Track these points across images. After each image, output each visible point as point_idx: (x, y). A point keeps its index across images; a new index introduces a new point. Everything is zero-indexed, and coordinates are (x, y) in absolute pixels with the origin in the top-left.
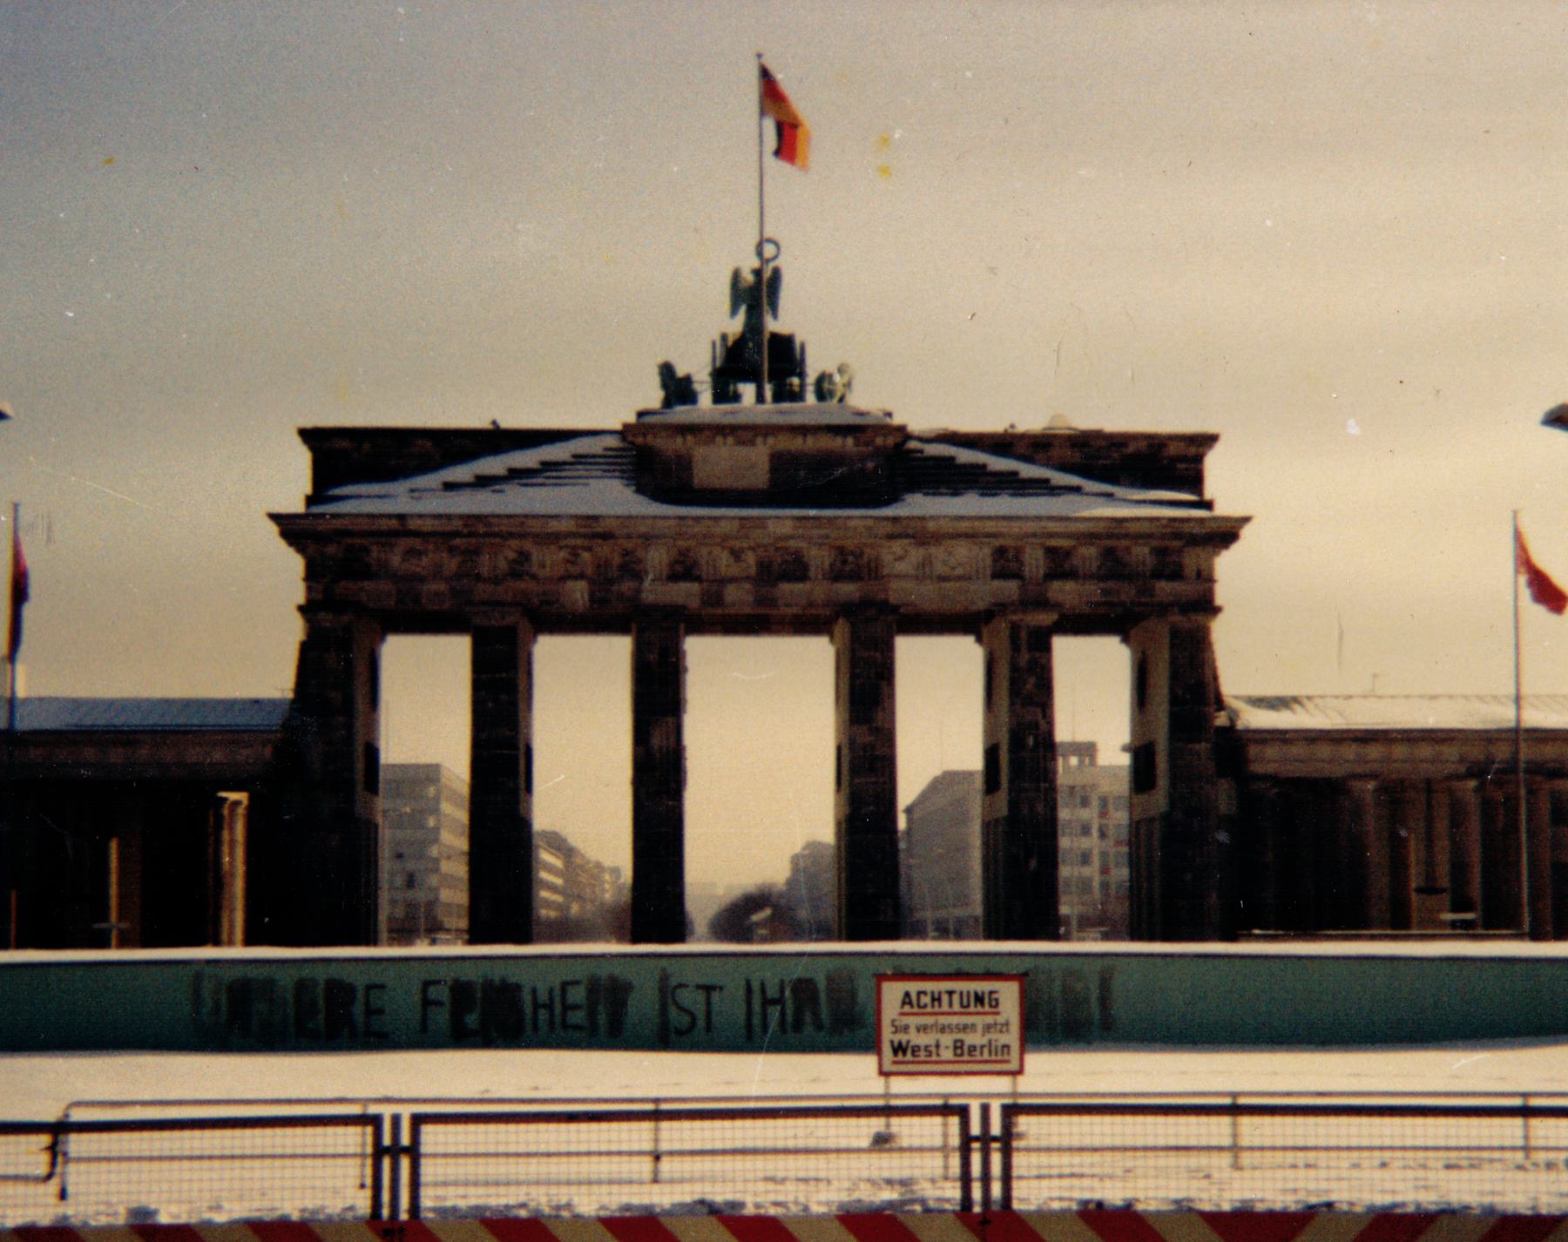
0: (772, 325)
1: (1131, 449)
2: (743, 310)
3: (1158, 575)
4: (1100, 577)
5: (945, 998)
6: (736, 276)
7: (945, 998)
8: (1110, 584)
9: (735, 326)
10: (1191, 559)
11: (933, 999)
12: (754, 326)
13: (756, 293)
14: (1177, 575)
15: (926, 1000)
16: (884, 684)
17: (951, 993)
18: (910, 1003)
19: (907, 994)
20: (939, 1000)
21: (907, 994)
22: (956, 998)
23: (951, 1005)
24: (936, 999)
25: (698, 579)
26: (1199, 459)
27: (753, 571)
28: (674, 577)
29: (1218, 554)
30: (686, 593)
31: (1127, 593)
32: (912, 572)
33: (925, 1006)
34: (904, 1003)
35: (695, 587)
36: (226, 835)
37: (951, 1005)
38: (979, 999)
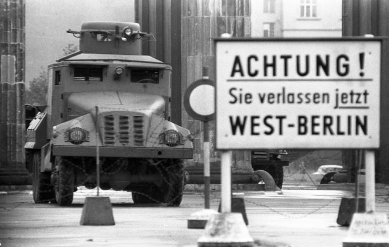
5: (280, 63)
7: (280, 63)
11: (266, 66)
15: (257, 66)
17: (286, 58)
18: (241, 71)
19: (237, 60)
20: (274, 65)
21: (237, 60)
22: (292, 63)
23: (286, 74)
24: (270, 65)
33: (256, 73)
34: (234, 72)
36: (9, 26)
37: (286, 74)
38: (322, 65)
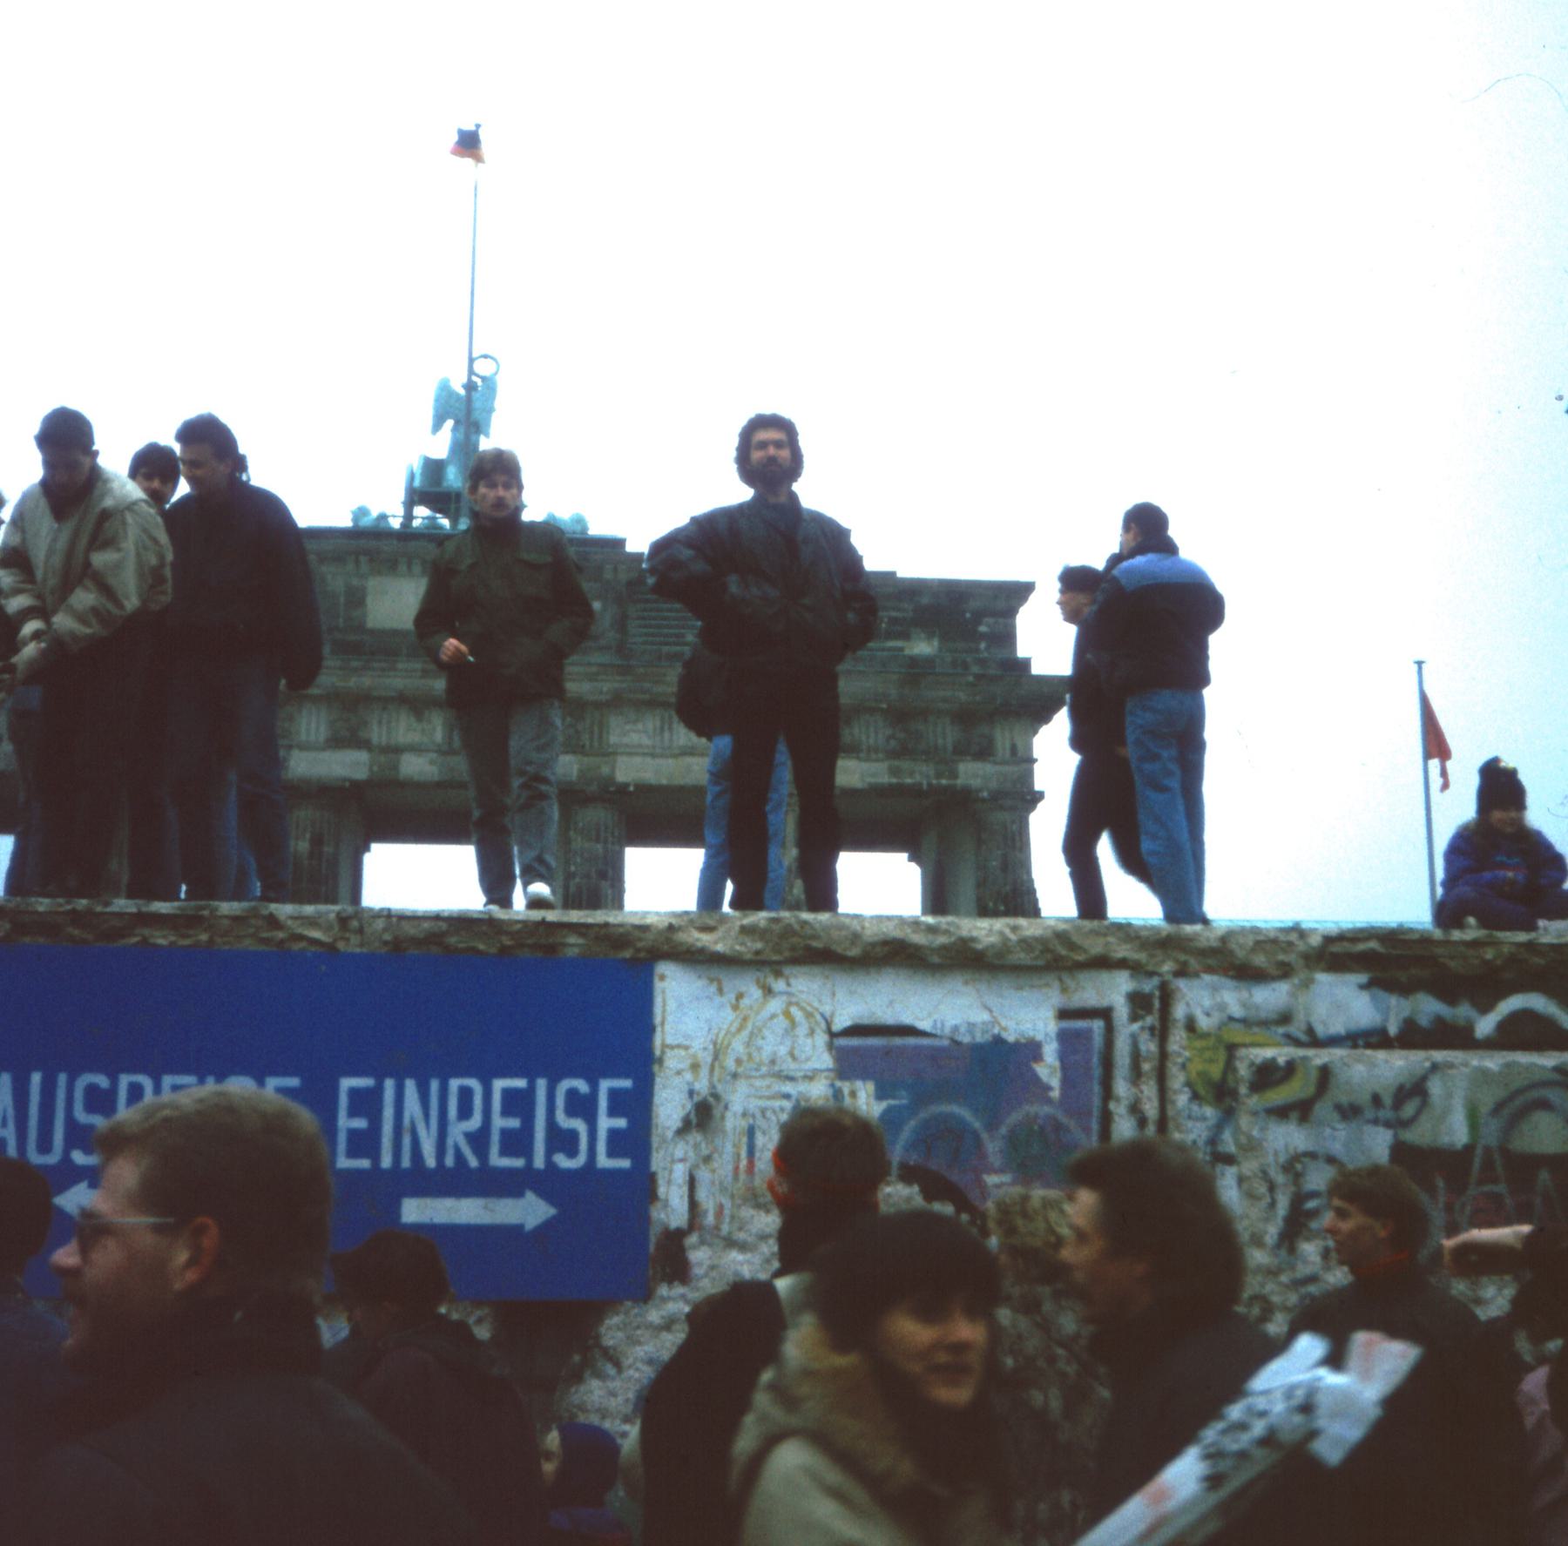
0: (485, 444)
1: (925, 601)
2: (450, 423)
3: (961, 751)
4: (893, 754)
6: (445, 388)
8: (906, 765)
9: (440, 445)
10: (1002, 738)
12: (464, 446)
13: (465, 409)
14: (984, 753)
16: (605, 885)
25: (364, 744)
26: (1011, 613)
27: (439, 736)
28: (336, 742)
29: (1035, 732)
30: (347, 765)
31: (920, 774)
32: (646, 741)
35: (362, 756)
